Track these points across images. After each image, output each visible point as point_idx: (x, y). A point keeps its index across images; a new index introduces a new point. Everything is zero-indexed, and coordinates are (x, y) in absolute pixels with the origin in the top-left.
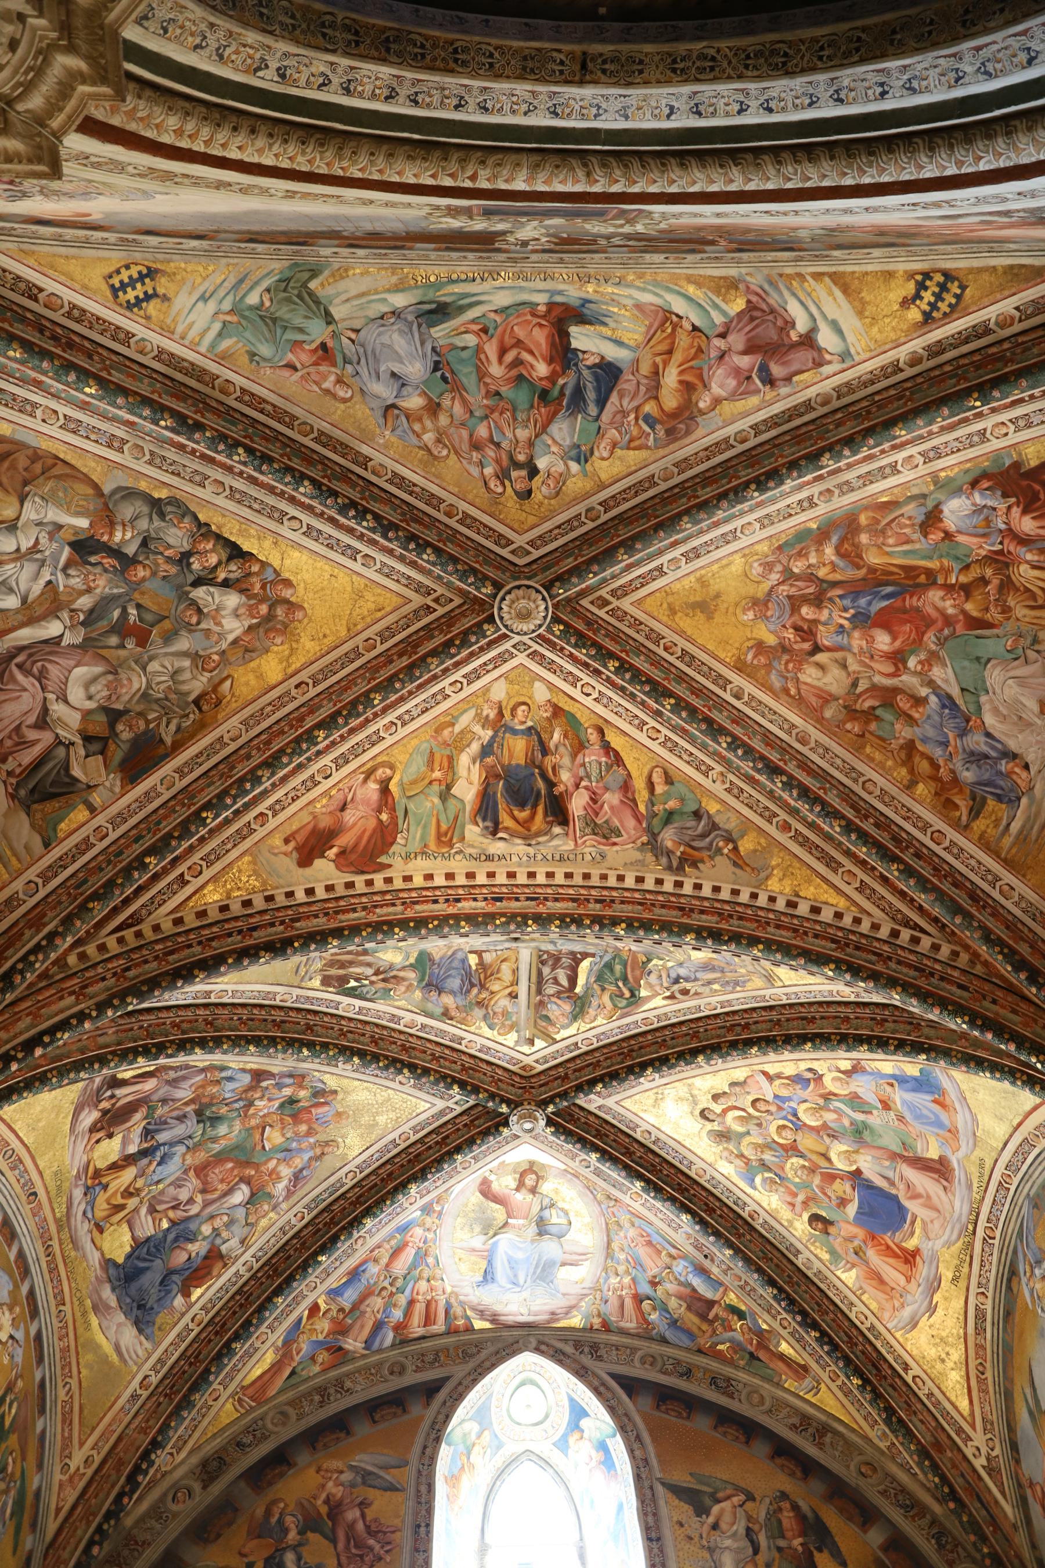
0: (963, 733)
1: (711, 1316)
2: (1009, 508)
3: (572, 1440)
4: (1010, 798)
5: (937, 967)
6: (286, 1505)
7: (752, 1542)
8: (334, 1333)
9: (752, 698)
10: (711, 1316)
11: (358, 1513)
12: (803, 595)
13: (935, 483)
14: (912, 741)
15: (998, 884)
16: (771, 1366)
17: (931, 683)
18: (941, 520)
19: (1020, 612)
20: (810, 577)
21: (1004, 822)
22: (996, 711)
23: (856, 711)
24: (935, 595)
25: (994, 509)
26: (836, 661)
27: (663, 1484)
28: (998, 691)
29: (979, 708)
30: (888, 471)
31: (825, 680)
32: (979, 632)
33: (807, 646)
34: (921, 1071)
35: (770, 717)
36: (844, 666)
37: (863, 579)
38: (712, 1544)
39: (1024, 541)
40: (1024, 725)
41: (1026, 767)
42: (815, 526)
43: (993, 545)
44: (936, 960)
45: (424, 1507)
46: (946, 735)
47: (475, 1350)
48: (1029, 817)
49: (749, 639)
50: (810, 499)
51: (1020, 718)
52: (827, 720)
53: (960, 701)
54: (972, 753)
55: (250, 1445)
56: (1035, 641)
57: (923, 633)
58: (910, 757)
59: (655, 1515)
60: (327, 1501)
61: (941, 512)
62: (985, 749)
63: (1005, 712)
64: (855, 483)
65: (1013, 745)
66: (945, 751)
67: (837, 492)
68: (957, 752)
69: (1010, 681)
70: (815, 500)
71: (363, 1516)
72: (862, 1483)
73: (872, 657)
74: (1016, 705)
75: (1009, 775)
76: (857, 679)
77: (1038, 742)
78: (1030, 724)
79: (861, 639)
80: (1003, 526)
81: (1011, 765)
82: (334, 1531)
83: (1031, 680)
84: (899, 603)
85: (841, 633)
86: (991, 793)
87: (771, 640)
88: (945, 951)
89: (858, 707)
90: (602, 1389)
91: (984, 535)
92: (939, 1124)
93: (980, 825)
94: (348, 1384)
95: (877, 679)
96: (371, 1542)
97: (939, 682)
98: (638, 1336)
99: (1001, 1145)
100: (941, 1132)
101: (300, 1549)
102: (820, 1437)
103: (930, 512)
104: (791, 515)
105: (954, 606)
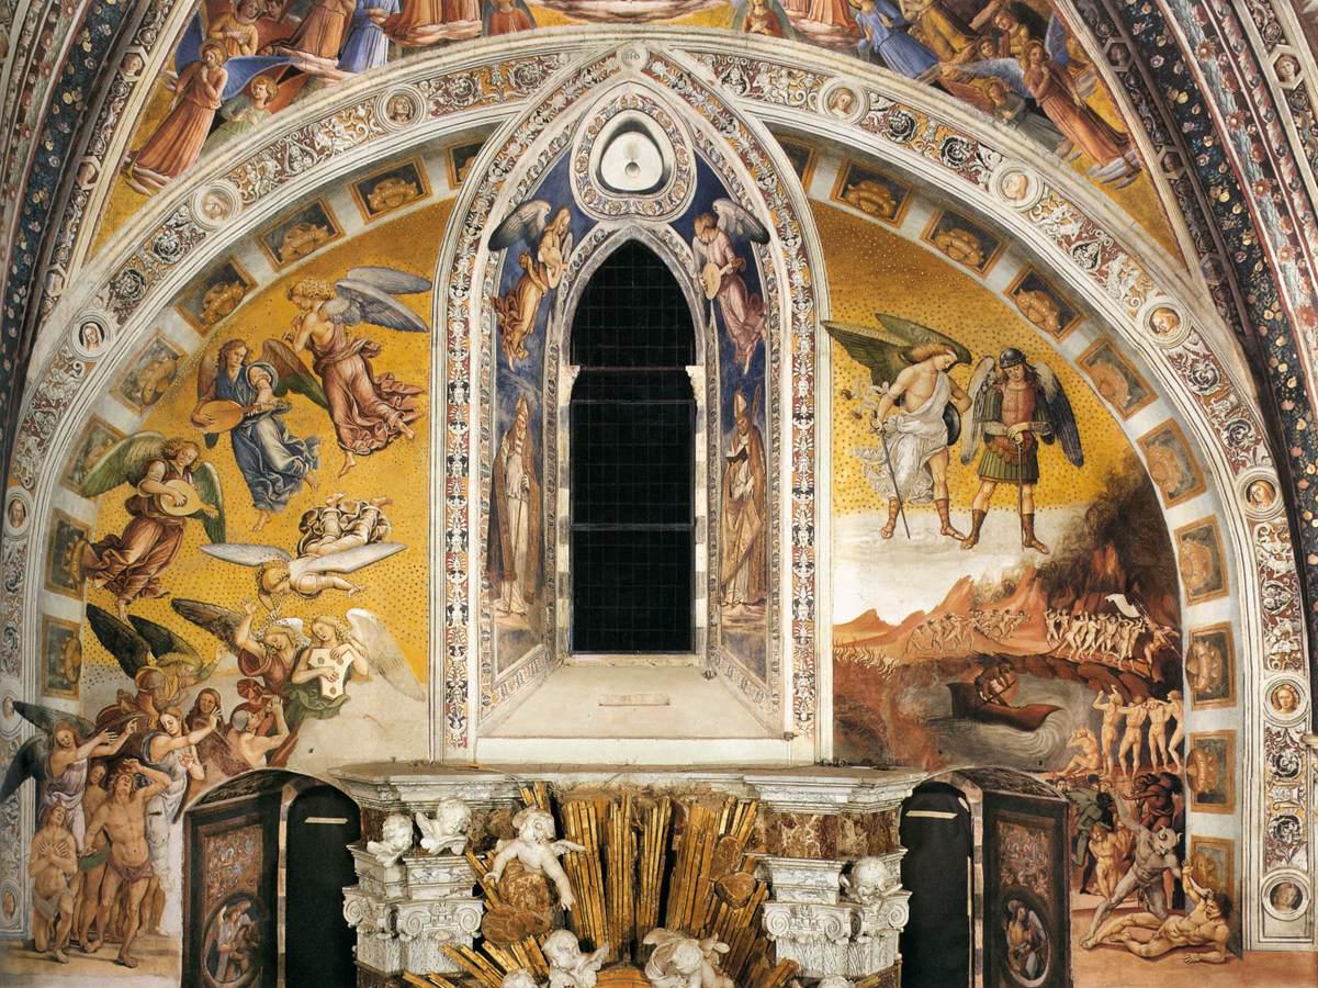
1: (976, 23)
3: (699, 226)
6: (249, 351)
7: (950, 425)
8: (272, 43)
10: (976, 23)
11: (360, 365)
16: (1062, 127)
27: (831, 331)
38: (889, 427)
45: (459, 358)
47: (537, 70)
55: (175, 252)
59: (810, 379)
60: (310, 346)
71: (368, 369)
72: (1149, 340)
82: (326, 390)
90: (754, 157)
94: (322, 139)
96: (383, 408)
98: (831, 46)
101: (280, 417)
102: (1104, 261)
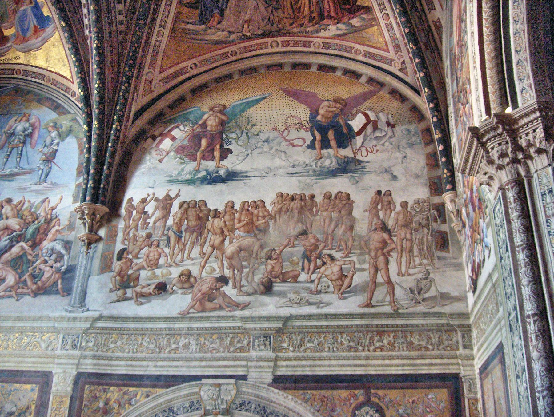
4: (202, 20)
5: (114, 18)
15: (162, 28)
21: (190, 21)
34: (48, 16)
40: (238, 15)
41: (219, 22)
44: (116, 16)
48: (197, 31)
51: (240, 12)
56: (276, 9)
65: (227, 12)
75: (212, 15)
78: (239, 18)
81: (217, 15)
83: (258, 13)
86: (201, 10)
88: (121, 18)
92: (24, 31)
93: (185, 10)
99: (33, 64)
100: (20, 33)
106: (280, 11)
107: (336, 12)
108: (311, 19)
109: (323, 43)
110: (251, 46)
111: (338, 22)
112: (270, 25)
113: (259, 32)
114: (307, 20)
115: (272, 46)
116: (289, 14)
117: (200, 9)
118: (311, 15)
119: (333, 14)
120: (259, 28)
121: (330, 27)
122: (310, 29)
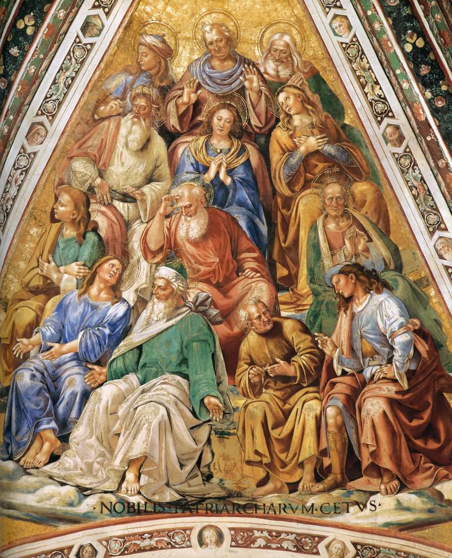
0: (81, 359)
2: (394, 381)
9: (88, 49)
12: (245, 109)
13: (419, 282)
14: (56, 291)
17: (142, 302)
18: (367, 291)
19: (257, 407)
20: (272, 121)
22: (121, 398)
23: (88, 204)
24: (261, 290)
25: (390, 361)
26: (156, 167)
28: (147, 396)
29: (119, 375)
30: (433, 218)
31: (126, 153)
32: (221, 357)
33: (173, 122)
35: (62, 80)
36: (149, 180)
37: (274, 192)
39: (352, 404)
40: (109, 441)
42: (347, 122)
43: (340, 362)
46: (73, 337)
49: (175, 35)
50: (388, 113)
52: (69, 168)
53: (123, 347)
54: (56, 378)
56: (222, 435)
57: (207, 281)
58: (36, 292)
61: (379, 292)
62: (66, 394)
63: (121, 412)
64: (410, 175)
65: (79, 433)
66: (51, 339)
67: (400, 150)
68: (53, 357)
69: (163, 411)
70: (386, 121)
73: (168, 216)
74: (133, 425)
75: (36, 435)
76: (134, 200)
77: (90, 466)
78: (111, 450)
79: (191, 197)
80: (367, 374)
81: (51, 436)
83: (170, 439)
84: (245, 243)
85: (197, 170)
87: (178, 69)
89: (94, 207)
91: (352, 349)
95: (138, 229)
97: (144, 314)
103: (377, 278)
104: (363, 86)
105: (250, 319)
106: (231, 442)
107: (396, 457)
108: (320, 474)
109: (355, 544)
110: (141, 535)
111: (402, 488)
112: (199, 479)
113: (170, 496)
114: (307, 475)
115: (201, 542)
116: (257, 452)
117: (7, 414)
118: (319, 462)
119: (386, 462)
120: (168, 485)
121: (377, 498)
122: (315, 500)
